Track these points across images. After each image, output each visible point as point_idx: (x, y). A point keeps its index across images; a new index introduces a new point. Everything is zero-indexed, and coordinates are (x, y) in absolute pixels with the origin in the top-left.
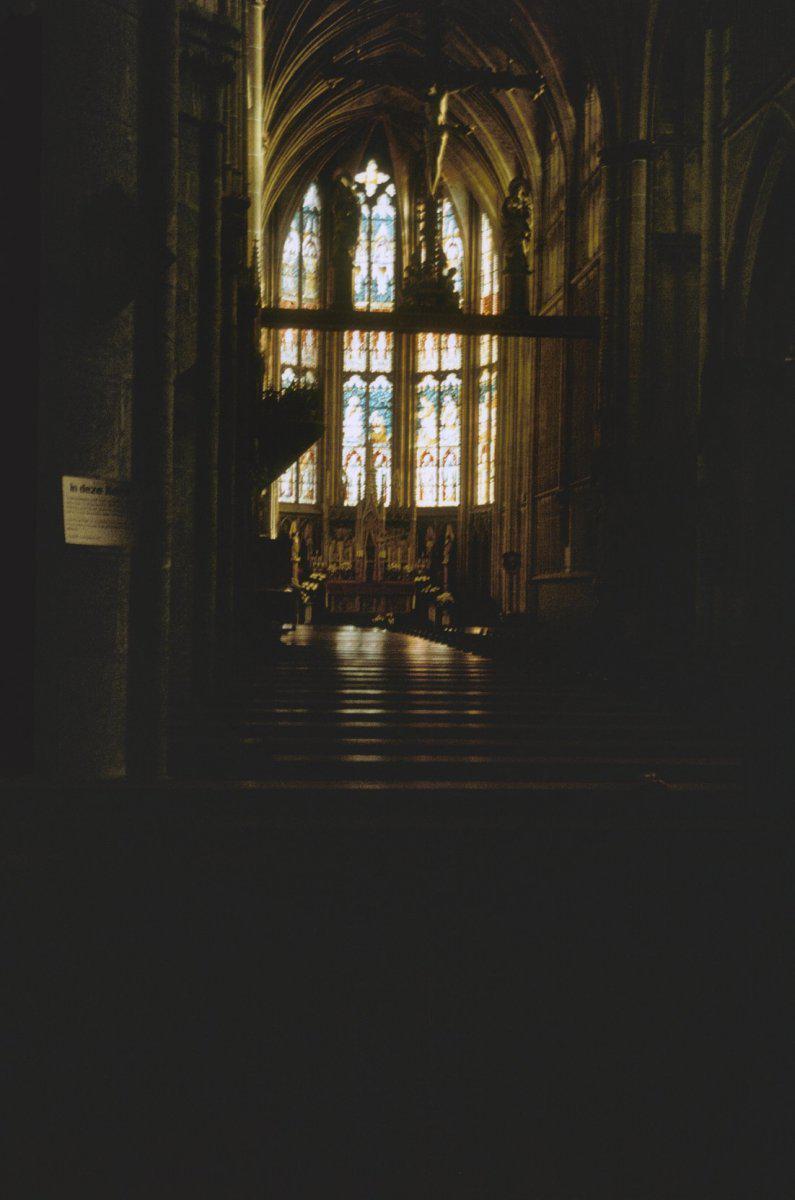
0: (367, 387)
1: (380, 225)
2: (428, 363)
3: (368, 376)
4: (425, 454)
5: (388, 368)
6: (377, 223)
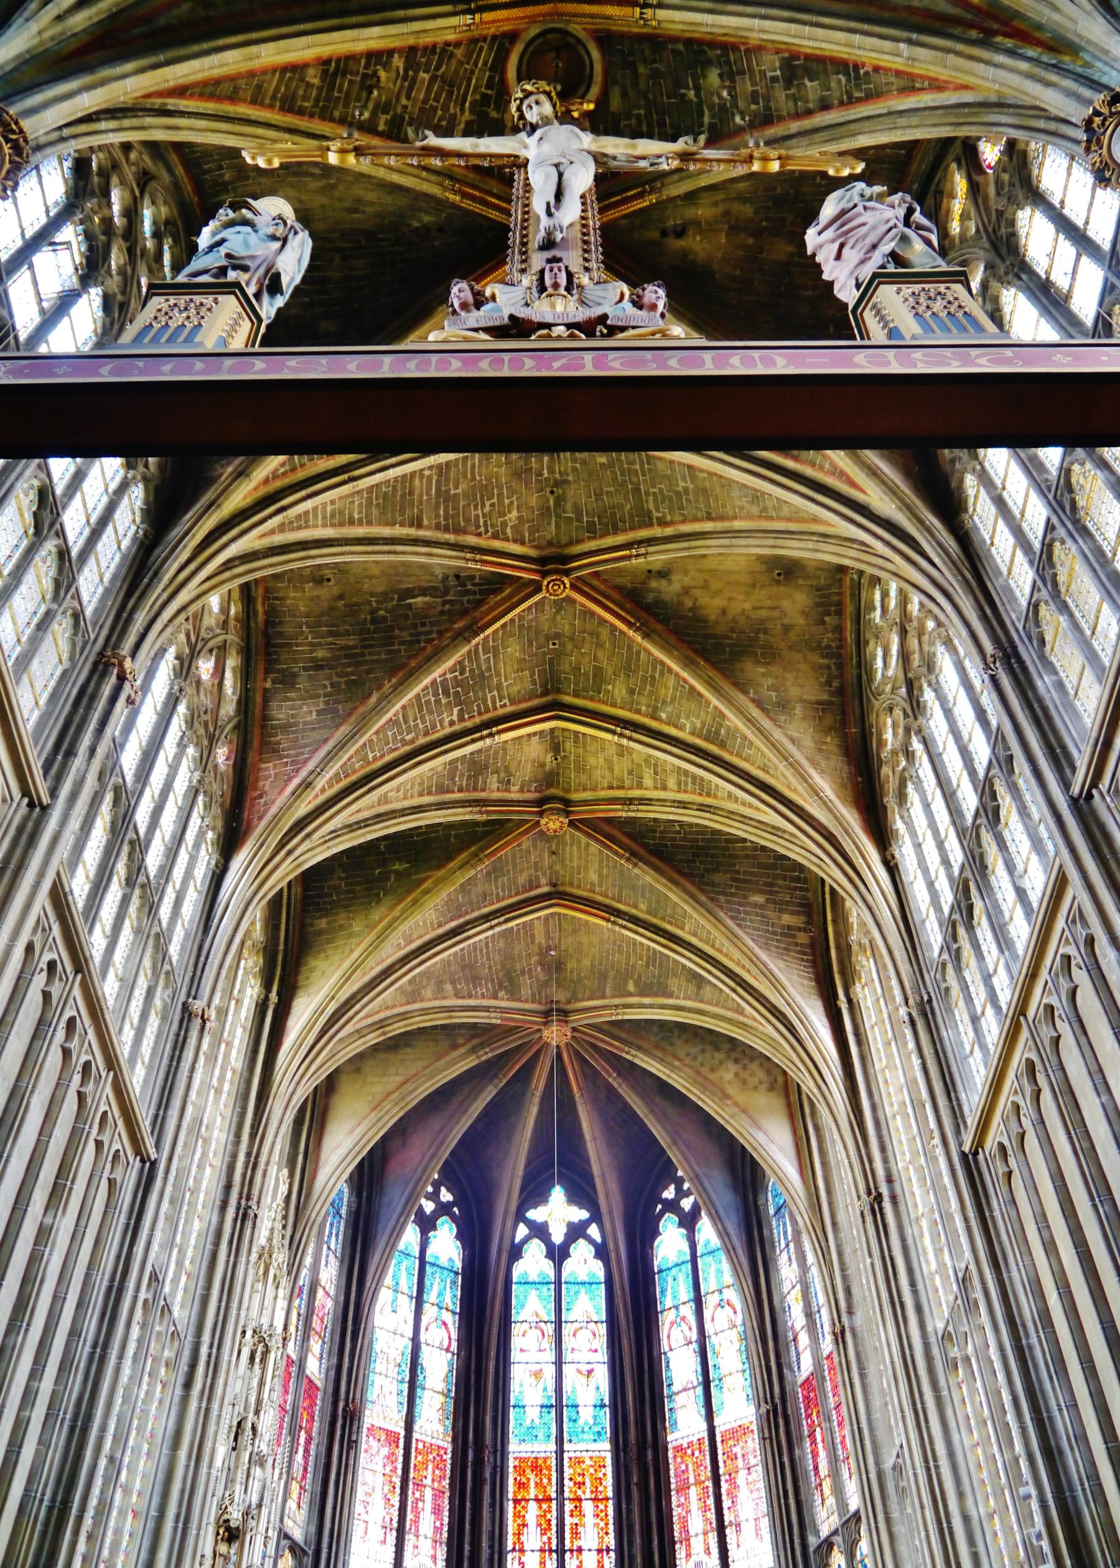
1: (577, 1293)
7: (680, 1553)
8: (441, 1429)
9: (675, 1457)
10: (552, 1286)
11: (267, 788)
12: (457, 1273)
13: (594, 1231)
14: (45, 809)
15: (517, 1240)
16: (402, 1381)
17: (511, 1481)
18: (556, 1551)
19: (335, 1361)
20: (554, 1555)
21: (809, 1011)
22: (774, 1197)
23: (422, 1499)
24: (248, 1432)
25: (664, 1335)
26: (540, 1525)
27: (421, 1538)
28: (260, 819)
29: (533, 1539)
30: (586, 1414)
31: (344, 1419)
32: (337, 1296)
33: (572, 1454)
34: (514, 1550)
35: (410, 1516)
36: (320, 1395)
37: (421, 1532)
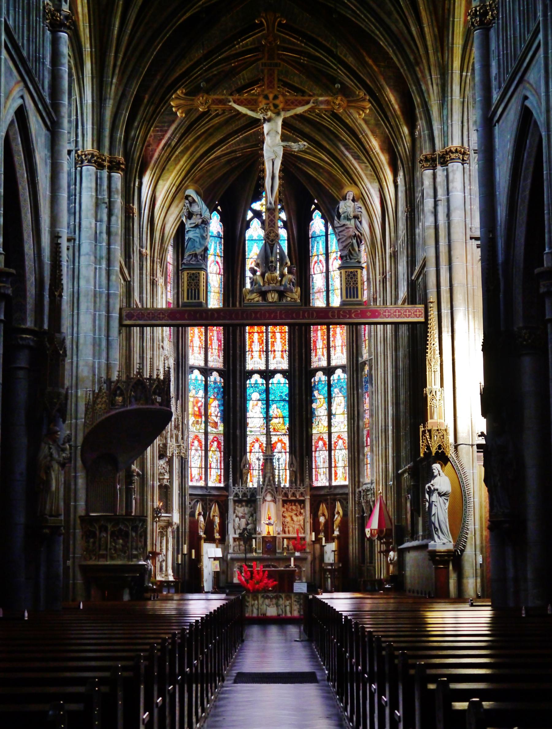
0: (267, 384)
2: (319, 360)
3: (267, 374)
5: (285, 365)
7: (313, 354)
11: (151, 142)
12: (221, 238)
14: (130, 282)
15: (248, 219)
18: (265, 351)
19: (176, 291)
20: (265, 353)
21: (372, 191)
24: (161, 348)
25: (312, 267)
26: (259, 342)
27: (214, 350)
28: (152, 157)
29: (256, 347)
32: (174, 263)
34: (249, 351)
35: (209, 342)
37: (213, 347)
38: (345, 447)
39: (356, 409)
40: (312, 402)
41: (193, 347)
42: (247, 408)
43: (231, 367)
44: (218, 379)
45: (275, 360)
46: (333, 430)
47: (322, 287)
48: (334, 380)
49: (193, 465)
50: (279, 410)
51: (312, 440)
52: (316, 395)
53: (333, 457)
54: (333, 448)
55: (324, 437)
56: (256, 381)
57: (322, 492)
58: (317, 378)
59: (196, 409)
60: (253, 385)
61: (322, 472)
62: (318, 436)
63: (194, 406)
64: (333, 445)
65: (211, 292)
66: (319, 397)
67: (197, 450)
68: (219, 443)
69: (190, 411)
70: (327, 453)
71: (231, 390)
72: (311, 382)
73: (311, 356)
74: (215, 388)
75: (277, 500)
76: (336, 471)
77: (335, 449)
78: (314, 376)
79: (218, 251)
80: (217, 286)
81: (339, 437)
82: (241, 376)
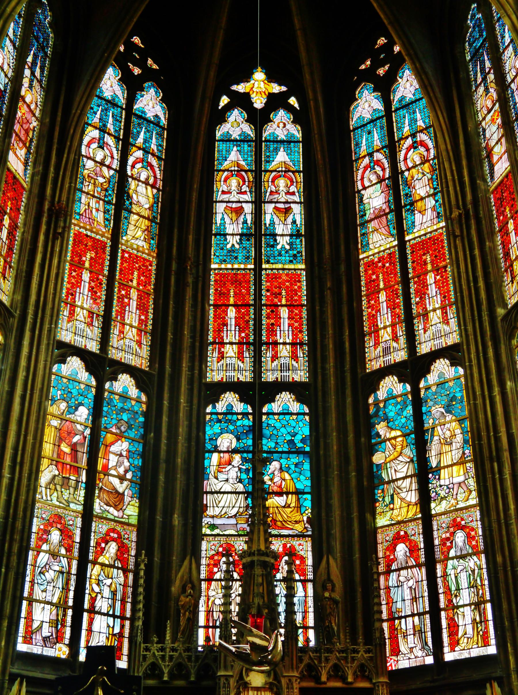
0: (257, 415)
1: (276, 150)
2: (387, 351)
4: (398, 539)
6: (272, 146)
7: (370, 342)
8: (146, 246)
9: (366, 271)
10: (253, 144)
12: (163, 128)
13: (293, 101)
16: (109, 203)
17: (212, 291)
18: (253, 344)
20: (252, 348)
22: (470, 45)
23: (128, 296)
30: (283, 242)
31: (50, 217)
33: (269, 272)
34: (214, 343)
35: (115, 308)
36: (25, 195)
37: (127, 321)
38: (473, 547)
39: (503, 430)
40: (372, 450)
41: (73, 306)
42: (204, 469)
43: (168, 368)
44: (134, 392)
45: (275, 363)
46: (436, 508)
47: (384, 207)
48: (427, 388)
49: (38, 594)
50: (287, 477)
51: (376, 543)
52: (382, 433)
53: (439, 581)
54: (438, 555)
55: (409, 532)
56: (230, 406)
57: (417, 685)
58: (382, 394)
59: (66, 449)
60: (220, 417)
61: (410, 626)
62: (391, 533)
63: (61, 440)
64: (437, 550)
65: (130, 212)
66: (388, 436)
67: (54, 555)
68: (122, 549)
69: (48, 449)
70: (421, 574)
71: (165, 419)
72: (368, 405)
73: (364, 347)
74: (123, 410)
75: (284, 681)
76: (453, 619)
77: (447, 558)
78: (375, 388)
79: (154, 147)
80: (147, 206)
81: (457, 526)
82: (191, 391)
